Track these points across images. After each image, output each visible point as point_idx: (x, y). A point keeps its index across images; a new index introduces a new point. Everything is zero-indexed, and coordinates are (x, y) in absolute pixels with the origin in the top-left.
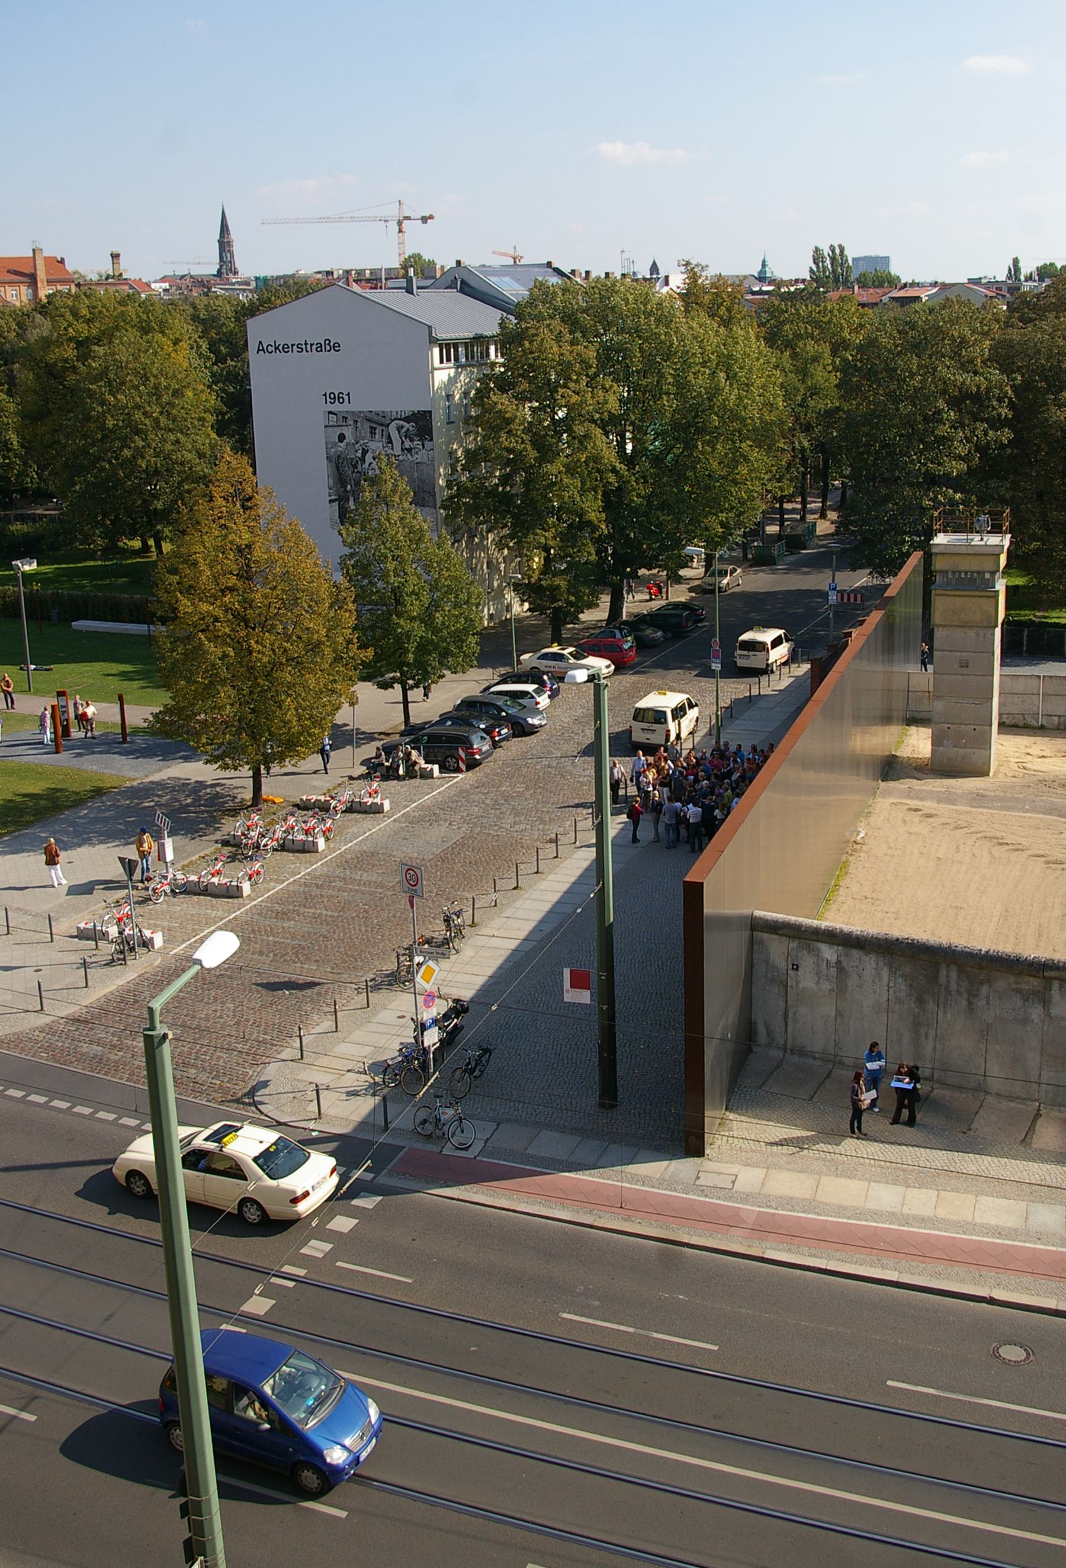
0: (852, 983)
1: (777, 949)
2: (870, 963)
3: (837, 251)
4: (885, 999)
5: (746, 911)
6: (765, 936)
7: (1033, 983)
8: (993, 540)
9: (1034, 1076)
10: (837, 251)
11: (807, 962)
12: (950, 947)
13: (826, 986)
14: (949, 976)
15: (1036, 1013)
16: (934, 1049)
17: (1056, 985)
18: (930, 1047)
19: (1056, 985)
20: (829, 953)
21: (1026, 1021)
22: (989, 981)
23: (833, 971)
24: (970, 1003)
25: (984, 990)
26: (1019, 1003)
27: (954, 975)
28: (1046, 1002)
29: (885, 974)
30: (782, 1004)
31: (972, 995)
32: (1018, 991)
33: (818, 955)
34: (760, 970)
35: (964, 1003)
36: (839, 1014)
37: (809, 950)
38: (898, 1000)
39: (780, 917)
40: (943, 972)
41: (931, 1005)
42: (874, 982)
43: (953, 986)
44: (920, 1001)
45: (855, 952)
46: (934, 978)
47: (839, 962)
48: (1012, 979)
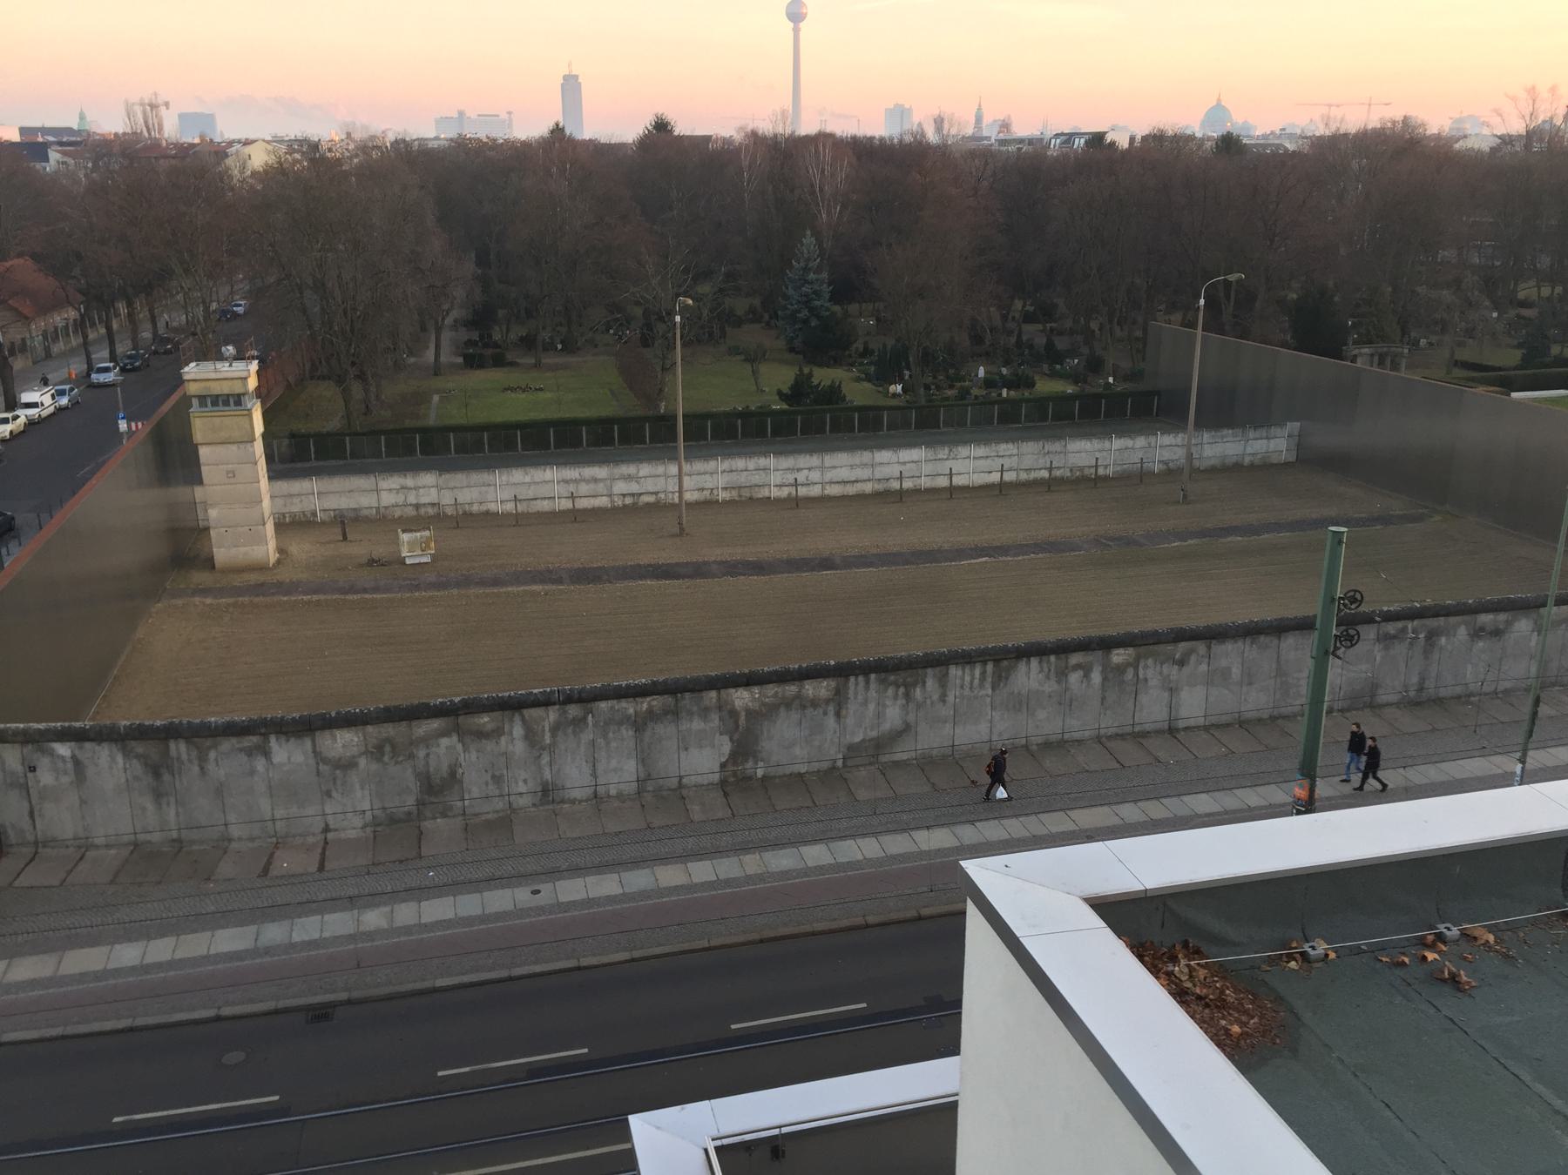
0: (90, 771)
8: (239, 366)
9: (268, 816)
11: (44, 763)
13: (65, 780)
15: (260, 764)
16: (177, 814)
18: (172, 813)
20: (63, 749)
21: (252, 772)
22: (215, 746)
23: (70, 766)
24: (202, 768)
25: (212, 755)
26: (243, 758)
27: (183, 746)
28: (267, 754)
29: (120, 759)
30: (26, 804)
31: (202, 759)
32: (241, 750)
33: (52, 753)
35: (196, 769)
36: (83, 802)
37: (43, 751)
38: (136, 778)
40: (172, 745)
41: (166, 777)
43: (184, 756)
44: (157, 775)
45: (88, 745)
47: (73, 757)
48: (234, 740)
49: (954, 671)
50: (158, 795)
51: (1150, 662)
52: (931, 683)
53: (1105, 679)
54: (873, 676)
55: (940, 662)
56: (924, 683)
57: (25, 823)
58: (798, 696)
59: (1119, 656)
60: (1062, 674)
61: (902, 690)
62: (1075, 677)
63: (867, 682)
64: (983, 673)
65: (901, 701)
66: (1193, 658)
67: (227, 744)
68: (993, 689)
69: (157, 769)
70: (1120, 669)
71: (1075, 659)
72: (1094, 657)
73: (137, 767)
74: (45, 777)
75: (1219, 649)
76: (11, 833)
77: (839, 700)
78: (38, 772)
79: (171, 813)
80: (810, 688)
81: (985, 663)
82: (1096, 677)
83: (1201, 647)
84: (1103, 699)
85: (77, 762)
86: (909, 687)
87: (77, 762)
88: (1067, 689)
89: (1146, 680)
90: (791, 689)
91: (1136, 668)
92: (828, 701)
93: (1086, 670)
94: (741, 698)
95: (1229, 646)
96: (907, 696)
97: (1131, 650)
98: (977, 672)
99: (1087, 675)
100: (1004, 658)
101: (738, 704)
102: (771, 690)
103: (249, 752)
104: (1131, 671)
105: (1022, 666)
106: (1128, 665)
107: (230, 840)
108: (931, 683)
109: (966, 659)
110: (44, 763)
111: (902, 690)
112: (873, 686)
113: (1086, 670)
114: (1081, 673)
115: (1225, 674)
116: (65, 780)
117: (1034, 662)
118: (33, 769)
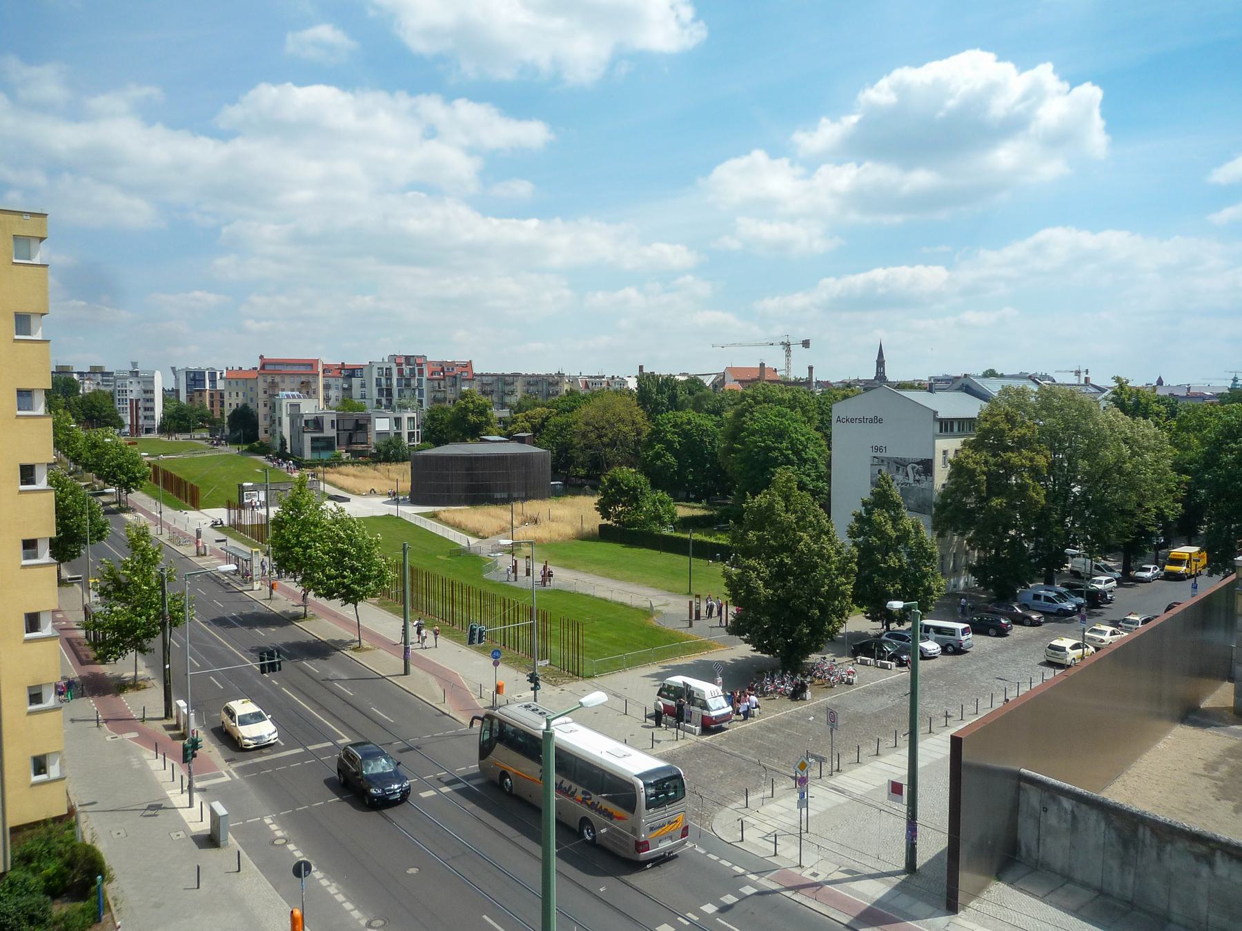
1: (1033, 798)
2: (1093, 816)
4: (1101, 842)
5: (1015, 768)
6: (1027, 786)
7: (1203, 849)
11: (1053, 808)
13: (1064, 826)
14: (1145, 834)
15: (1205, 871)
17: (1218, 854)
19: (1218, 854)
20: (1067, 804)
21: (1197, 875)
23: (1069, 817)
25: (1169, 848)
28: (1211, 865)
29: (1103, 825)
31: (1160, 850)
33: (1060, 803)
34: (1023, 807)
35: (1154, 854)
36: (1073, 847)
39: (1068, 786)
40: (1141, 830)
41: (1132, 851)
42: (1095, 830)
43: (1148, 841)
45: (1083, 806)
47: (1073, 811)
48: (1187, 844)
50: (1124, 864)
57: (1033, 844)
67: (1181, 845)
73: (1113, 834)
74: (1052, 819)
76: (1023, 847)
78: (1049, 813)
79: (1130, 879)
85: (1074, 817)
87: (1074, 817)
103: (1199, 857)
107: (1170, 921)
110: (1053, 808)
116: (1064, 826)
118: (1045, 810)
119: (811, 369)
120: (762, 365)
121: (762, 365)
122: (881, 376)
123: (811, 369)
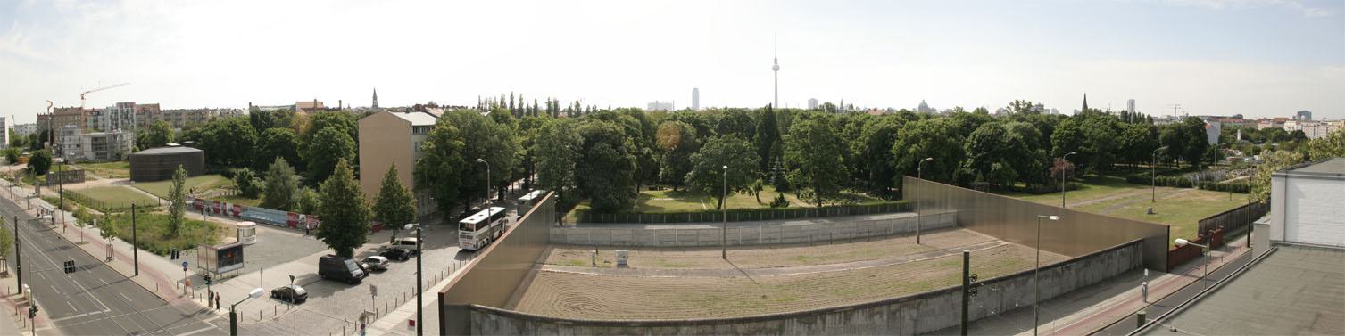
3: (552, 105)
7: (552, 326)
10: (552, 105)
12: (1108, 113)
14: (528, 324)
27: (530, 324)
31: (536, 330)
40: (527, 324)
46: (524, 325)
49: (828, 318)
51: (905, 309)
52: (819, 321)
53: (888, 318)
54: (795, 320)
55: (822, 313)
56: (816, 322)
58: (764, 328)
59: (893, 307)
60: (872, 316)
61: (807, 326)
62: (877, 317)
63: (793, 322)
64: (840, 317)
65: (807, 330)
66: (921, 307)
67: (545, 326)
68: (845, 323)
69: (521, 330)
70: (894, 313)
71: (876, 309)
72: (885, 308)
75: (930, 301)
77: (781, 329)
80: (769, 324)
81: (840, 313)
82: (885, 317)
83: (924, 301)
84: (888, 326)
86: (810, 324)
88: (874, 323)
89: (904, 317)
90: (762, 325)
91: (900, 310)
92: (776, 330)
93: (880, 313)
94: (741, 328)
95: (935, 300)
96: (809, 328)
97: (898, 305)
98: (838, 316)
99: (881, 317)
100: (848, 312)
101: (739, 330)
102: (754, 325)
104: (898, 314)
105: (856, 314)
106: (897, 311)
108: (819, 321)
109: (832, 311)
111: (807, 326)
112: (795, 323)
113: (880, 313)
114: (879, 316)
115: (934, 311)
117: (860, 311)
119: (340, 101)
120: (315, 100)
121: (315, 100)
122: (375, 106)
123: (340, 101)
